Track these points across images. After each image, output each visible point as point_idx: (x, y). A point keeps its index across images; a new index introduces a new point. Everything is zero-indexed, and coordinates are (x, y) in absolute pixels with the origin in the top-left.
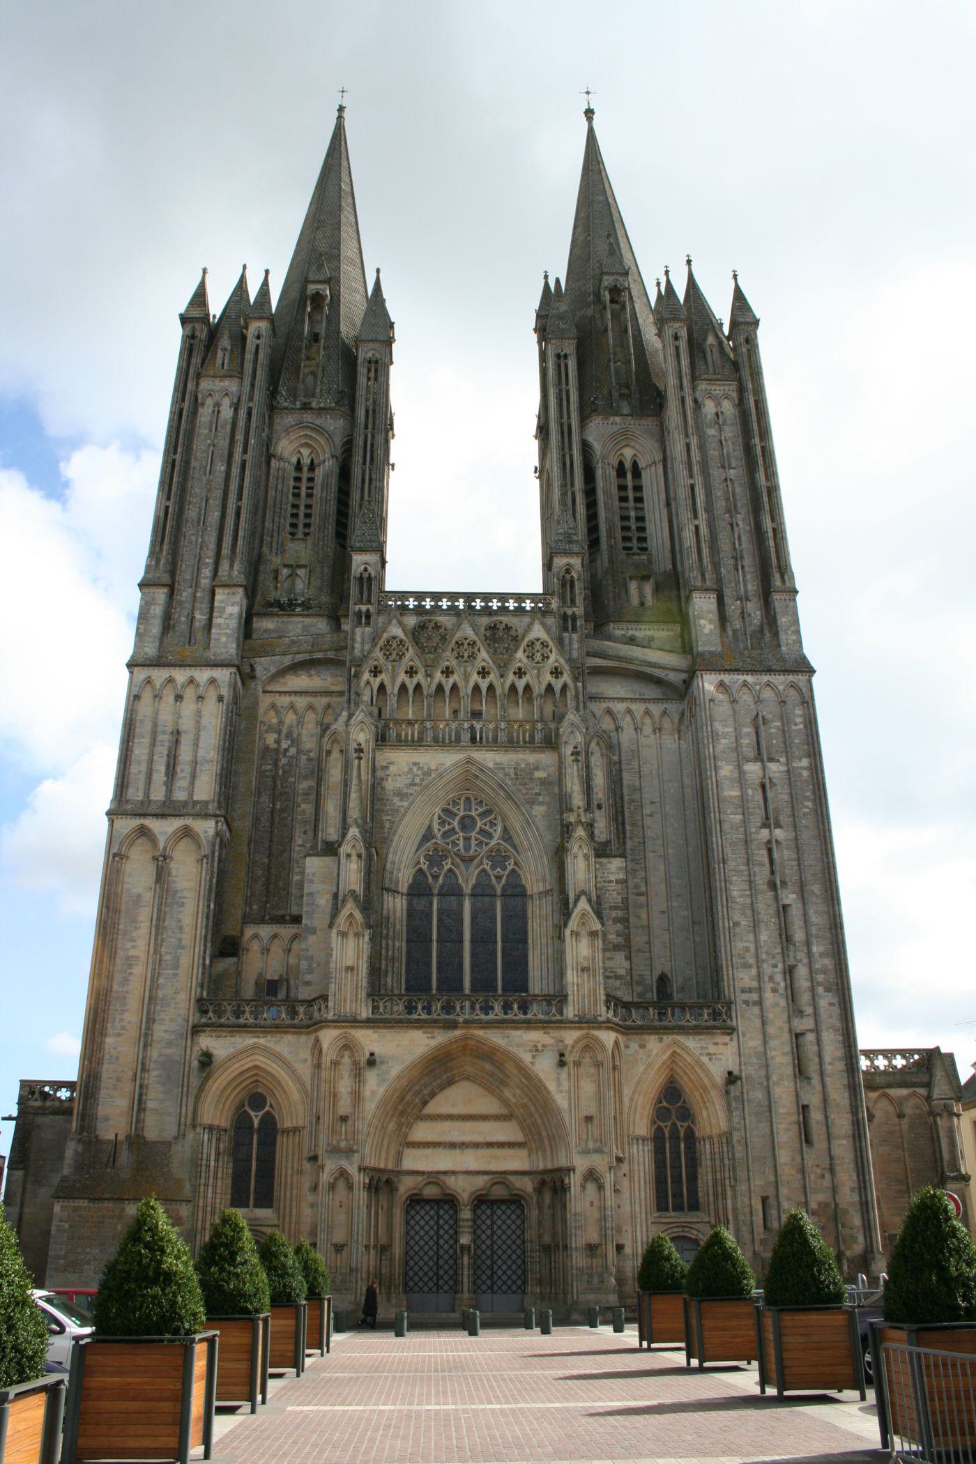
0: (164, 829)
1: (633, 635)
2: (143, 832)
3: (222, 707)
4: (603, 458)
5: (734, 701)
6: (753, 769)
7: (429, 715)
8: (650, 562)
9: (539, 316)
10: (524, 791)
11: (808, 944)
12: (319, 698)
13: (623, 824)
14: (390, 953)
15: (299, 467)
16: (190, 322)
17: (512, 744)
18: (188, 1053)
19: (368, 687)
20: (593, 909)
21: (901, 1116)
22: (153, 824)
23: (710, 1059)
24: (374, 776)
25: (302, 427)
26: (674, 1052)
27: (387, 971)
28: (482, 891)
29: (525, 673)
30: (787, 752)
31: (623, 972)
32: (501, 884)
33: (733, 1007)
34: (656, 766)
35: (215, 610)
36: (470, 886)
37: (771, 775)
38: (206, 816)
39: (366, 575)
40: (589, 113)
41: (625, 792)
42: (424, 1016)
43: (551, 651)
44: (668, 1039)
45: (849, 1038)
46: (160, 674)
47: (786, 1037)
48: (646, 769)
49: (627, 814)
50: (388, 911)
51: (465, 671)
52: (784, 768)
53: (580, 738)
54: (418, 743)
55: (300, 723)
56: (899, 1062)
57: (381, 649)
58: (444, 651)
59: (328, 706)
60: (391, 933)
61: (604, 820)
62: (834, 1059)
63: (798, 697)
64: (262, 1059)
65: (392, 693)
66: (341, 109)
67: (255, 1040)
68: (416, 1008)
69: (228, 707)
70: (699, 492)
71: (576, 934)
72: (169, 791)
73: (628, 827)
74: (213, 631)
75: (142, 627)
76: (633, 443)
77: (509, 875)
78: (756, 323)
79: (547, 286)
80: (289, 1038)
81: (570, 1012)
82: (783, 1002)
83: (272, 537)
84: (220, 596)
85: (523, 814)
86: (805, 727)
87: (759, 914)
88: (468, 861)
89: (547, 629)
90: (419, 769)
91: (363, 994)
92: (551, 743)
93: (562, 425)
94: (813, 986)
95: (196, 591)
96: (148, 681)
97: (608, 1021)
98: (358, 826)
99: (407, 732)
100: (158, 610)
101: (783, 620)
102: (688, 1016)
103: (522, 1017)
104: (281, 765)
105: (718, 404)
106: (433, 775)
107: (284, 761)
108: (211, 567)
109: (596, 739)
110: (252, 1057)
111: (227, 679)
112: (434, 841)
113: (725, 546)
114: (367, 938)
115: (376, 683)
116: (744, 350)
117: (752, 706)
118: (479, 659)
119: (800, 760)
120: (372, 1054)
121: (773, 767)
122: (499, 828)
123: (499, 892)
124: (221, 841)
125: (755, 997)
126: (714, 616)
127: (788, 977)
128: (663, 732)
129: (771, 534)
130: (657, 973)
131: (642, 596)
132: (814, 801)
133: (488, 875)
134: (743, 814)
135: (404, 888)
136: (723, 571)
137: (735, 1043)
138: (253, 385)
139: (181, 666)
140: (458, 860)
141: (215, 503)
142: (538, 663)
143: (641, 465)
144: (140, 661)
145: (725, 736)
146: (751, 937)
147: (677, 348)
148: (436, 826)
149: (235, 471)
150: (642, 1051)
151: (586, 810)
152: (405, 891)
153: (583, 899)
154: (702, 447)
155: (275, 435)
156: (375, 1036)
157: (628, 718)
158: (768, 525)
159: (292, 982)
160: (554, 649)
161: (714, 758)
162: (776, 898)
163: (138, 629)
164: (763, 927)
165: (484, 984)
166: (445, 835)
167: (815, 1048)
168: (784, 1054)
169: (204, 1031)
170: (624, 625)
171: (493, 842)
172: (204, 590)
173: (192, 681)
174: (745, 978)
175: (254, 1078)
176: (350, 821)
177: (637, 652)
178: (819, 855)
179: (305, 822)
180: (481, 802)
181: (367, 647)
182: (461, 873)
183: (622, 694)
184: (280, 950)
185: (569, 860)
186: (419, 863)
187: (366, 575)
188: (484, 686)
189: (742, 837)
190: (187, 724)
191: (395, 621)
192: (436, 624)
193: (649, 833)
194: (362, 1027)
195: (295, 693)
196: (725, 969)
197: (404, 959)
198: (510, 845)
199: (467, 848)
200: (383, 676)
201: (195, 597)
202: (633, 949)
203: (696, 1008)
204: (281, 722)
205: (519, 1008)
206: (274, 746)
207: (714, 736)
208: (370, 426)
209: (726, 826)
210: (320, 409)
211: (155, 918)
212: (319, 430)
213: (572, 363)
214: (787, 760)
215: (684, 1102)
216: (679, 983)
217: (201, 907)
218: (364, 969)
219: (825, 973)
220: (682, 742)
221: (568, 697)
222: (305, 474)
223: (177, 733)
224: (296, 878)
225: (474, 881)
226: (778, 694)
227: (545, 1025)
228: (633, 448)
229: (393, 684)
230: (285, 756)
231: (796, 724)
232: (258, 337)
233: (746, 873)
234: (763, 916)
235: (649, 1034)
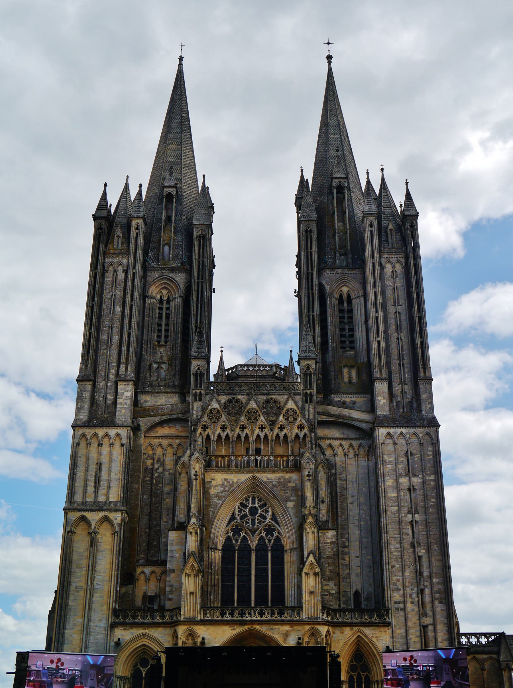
0: (94, 517)
1: (344, 401)
2: (83, 519)
3: (124, 449)
4: (331, 294)
5: (395, 444)
6: (404, 481)
7: (233, 453)
8: (356, 355)
9: (297, 198)
10: (283, 494)
11: (430, 577)
12: (174, 440)
13: (337, 508)
14: (213, 582)
15: (161, 301)
16: (99, 219)
17: (276, 468)
18: (109, 638)
19: (201, 437)
20: (316, 560)
21: (483, 669)
22: (89, 515)
23: (377, 640)
24: (204, 488)
25: (163, 278)
26: (359, 635)
27: (211, 592)
28: (261, 548)
29: (284, 428)
30: (423, 471)
31: (333, 592)
32: (271, 544)
33: (390, 611)
34: (355, 475)
35: (118, 394)
36: (255, 545)
37: (414, 484)
38: (116, 511)
39: (199, 372)
40: (329, 58)
41: (338, 490)
42: (230, 618)
43: (298, 416)
44: (355, 629)
45: (451, 629)
46: (90, 431)
47: (418, 628)
48: (350, 477)
49: (339, 503)
50: (212, 560)
51: (252, 428)
52: (420, 481)
53: (312, 466)
54: (227, 468)
55: (164, 454)
56: (483, 640)
58: (241, 416)
59: (180, 444)
60: (213, 571)
61: (325, 508)
62: (443, 640)
63: (430, 439)
64: (147, 640)
65: (213, 440)
66: (181, 58)
67: (144, 631)
68: (225, 614)
69: (127, 449)
70: (381, 320)
71: (307, 574)
72: (96, 497)
73: (339, 510)
74: (118, 406)
75: (79, 404)
76: (348, 284)
77: (274, 539)
78: (417, 215)
79: (302, 177)
80: (161, 630)
81: (304, 616)
82: (416, 609)
83: (147, 345)
84: (121, 386)
85: (282, 506)
86: (434, 457)
87: (405, 561)
88: (253, 532)
89: (296, 403)
90: (228, 482)
91: (198, 607)
92: (297, 467)
93: (308, 274)
94: (432, 600)
95: (107, 383)
96: (84, 435)
97: (324, 621)
98: (195, 517)
99: (222, 462)
100: (87, 395)
101: (424, 396)
102: (366, 617)
103: (280, 618)
104: (155, 477)
105: (393, 267)
106: (235, 486)
107: (156, 475)
108: (115, 368)
109: (321, 464)
110: (142, 640)
111: (125, 434)
112: (236, 520)
113: (394, 352)
114: (200, 577)
115: (205, 435)
116: (410, 232)
117: (405, 446)
118: (260, 421)
119: (430, 475)
120: (203, 639)
121: (415, 480)
122: (270, 513)
123: (270, 548)
124: (125, 522)
125: (402, 606)
126: (387, 395)
127: (420, 595)
128: (359, 456)
129: (419, 346)
130: (353, 590)
131: (350, 377)
132: (437, 499)
133: (264, 539)
134: (398, 506)
135: (220, 547)
136: (393, 368)
137: (390, 631)
138: (135, 258)
139: (100, 427)
140: (248, 531)
141: (116, 330)
142: (291, 422)
143: (353, 296)
144: (80, 423)
145: (390, 462)
146: (400, 574)
147: (371, 232)
148: (237, 513)
149: (127, 312)
150: (342, 635)
151: (314, 507)
152: (221, 548)
153: (311, 556)
154: (383, 293)
155: (148, 284)
156: (205, 629)
157: (340, 449)
158: (418, 341)
159: (162, 597)
160: (299, 415)
161: (384, 475)
162: (414, 552)
163: (77, 405)
164: (406, 567)
165: (261, 600)
166: (242, 518)
167: (433, 634)
168: (417, 637)
169: (117, 627)
170: (340, 395)
171: (267, 521)
172: (112, 382)
173: (107, 435)
174: (397, 596)
175: (143, 651)
176: (191, 514)
177: (346, 412)
178: (438, 529)
179: (168, 509)
181: (200, 414)
182: (250, 538)
183: (337, 436)
184: (155, 579)
185: (305, 534)
186: (228, 533)
187: (199, 372)
188: (262, 436)
189: (397, 519)
190: (105, 460)
191: (214, 400)
192: (237, 400)
193: (351, 513)
194: (198, 625)
195: (162, 437)
196: (386, 592)
197: (220, 585)
199: (253, 524)
200: (209, 430)
201: (107, 385)
202: (341, 577)
203: (370, 612)
204: (154, 453)
205: (278, 614)
206: (151, 467)
207: (384, 463)
208: (200, 277)
209: (389, 513)
210: (172, 268)
211: (90, 565)
212: (172, 280)
213: (314, 236)
214: (423, 476)
215: (365, 662)
216: (365, 596)
217: (114, 560)
218: (199, 594)
219: (439, 594)
220: (370, 462)
221: (307, 441)
222: (165, 306)
223: (100, 465)
224: (163, 540)
225: (257, 543)
226: (419, 439)
227: (291, 623)
228: (348, 287)
229: (214, 436)
230: (156, 472)
231: (428, 456)
232: (137, 229)
233: (399, 539)
234: (407, 562)
235: (346, 626)
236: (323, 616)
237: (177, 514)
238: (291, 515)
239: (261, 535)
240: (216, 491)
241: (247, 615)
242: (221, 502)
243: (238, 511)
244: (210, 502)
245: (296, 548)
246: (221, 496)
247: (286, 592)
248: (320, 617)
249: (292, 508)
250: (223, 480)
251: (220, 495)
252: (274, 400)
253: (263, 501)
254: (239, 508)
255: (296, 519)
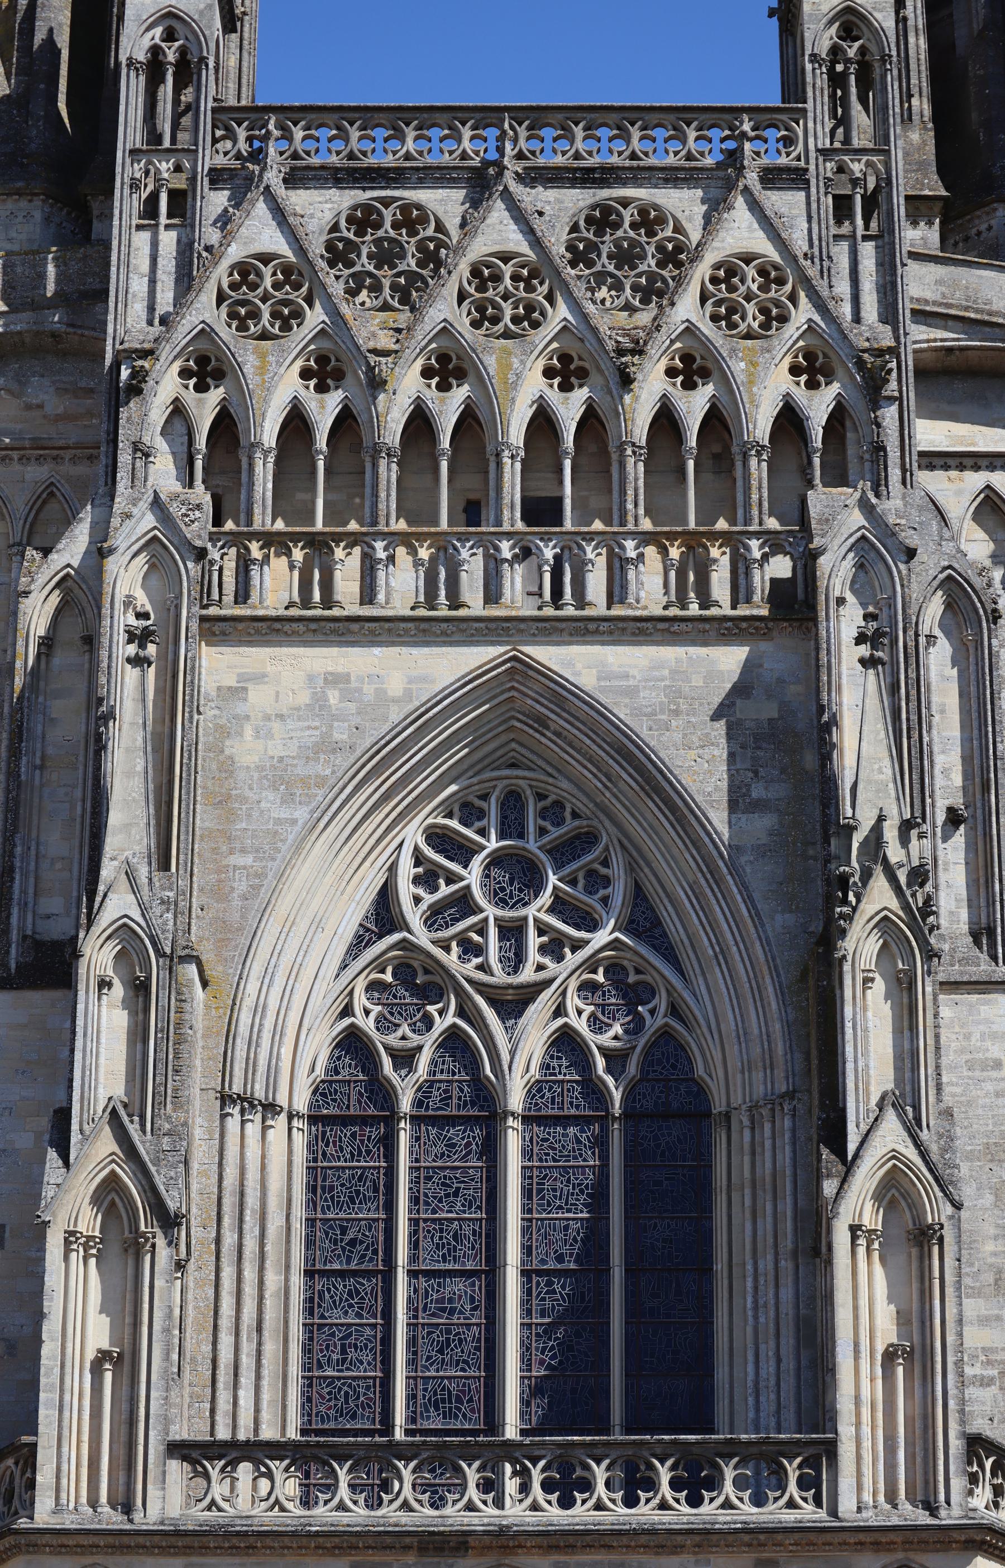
57: (221, 298)
60: (251, 1245)
90: (347, 696)
122: (619, 892)
148: (405, 889)
151: (906, 827)
152: (302, 1103)
176: (108, 871)
180: (559, 805)
186: (347, 1011)
198: (655, 948)
205: (675, 1485)
221: (851, 451)
236: (971, 1493)
237: (24, 891)
238: (756, 896)
239: (560, 1022)
240: (276, 749)
241: (473, 1493)
242: (302, 814)
243: (417, 880)
244: (231, 816)
245: (790, 1095)
246: (304, 781)
247: (721, 1374)
248: (955, 1498)
249: (762, 852)
250: (321, 682)
251: (299, 771)
252: (643, 212)
253: (575, 815)
254: (419, 859)
255: (790, 919)
